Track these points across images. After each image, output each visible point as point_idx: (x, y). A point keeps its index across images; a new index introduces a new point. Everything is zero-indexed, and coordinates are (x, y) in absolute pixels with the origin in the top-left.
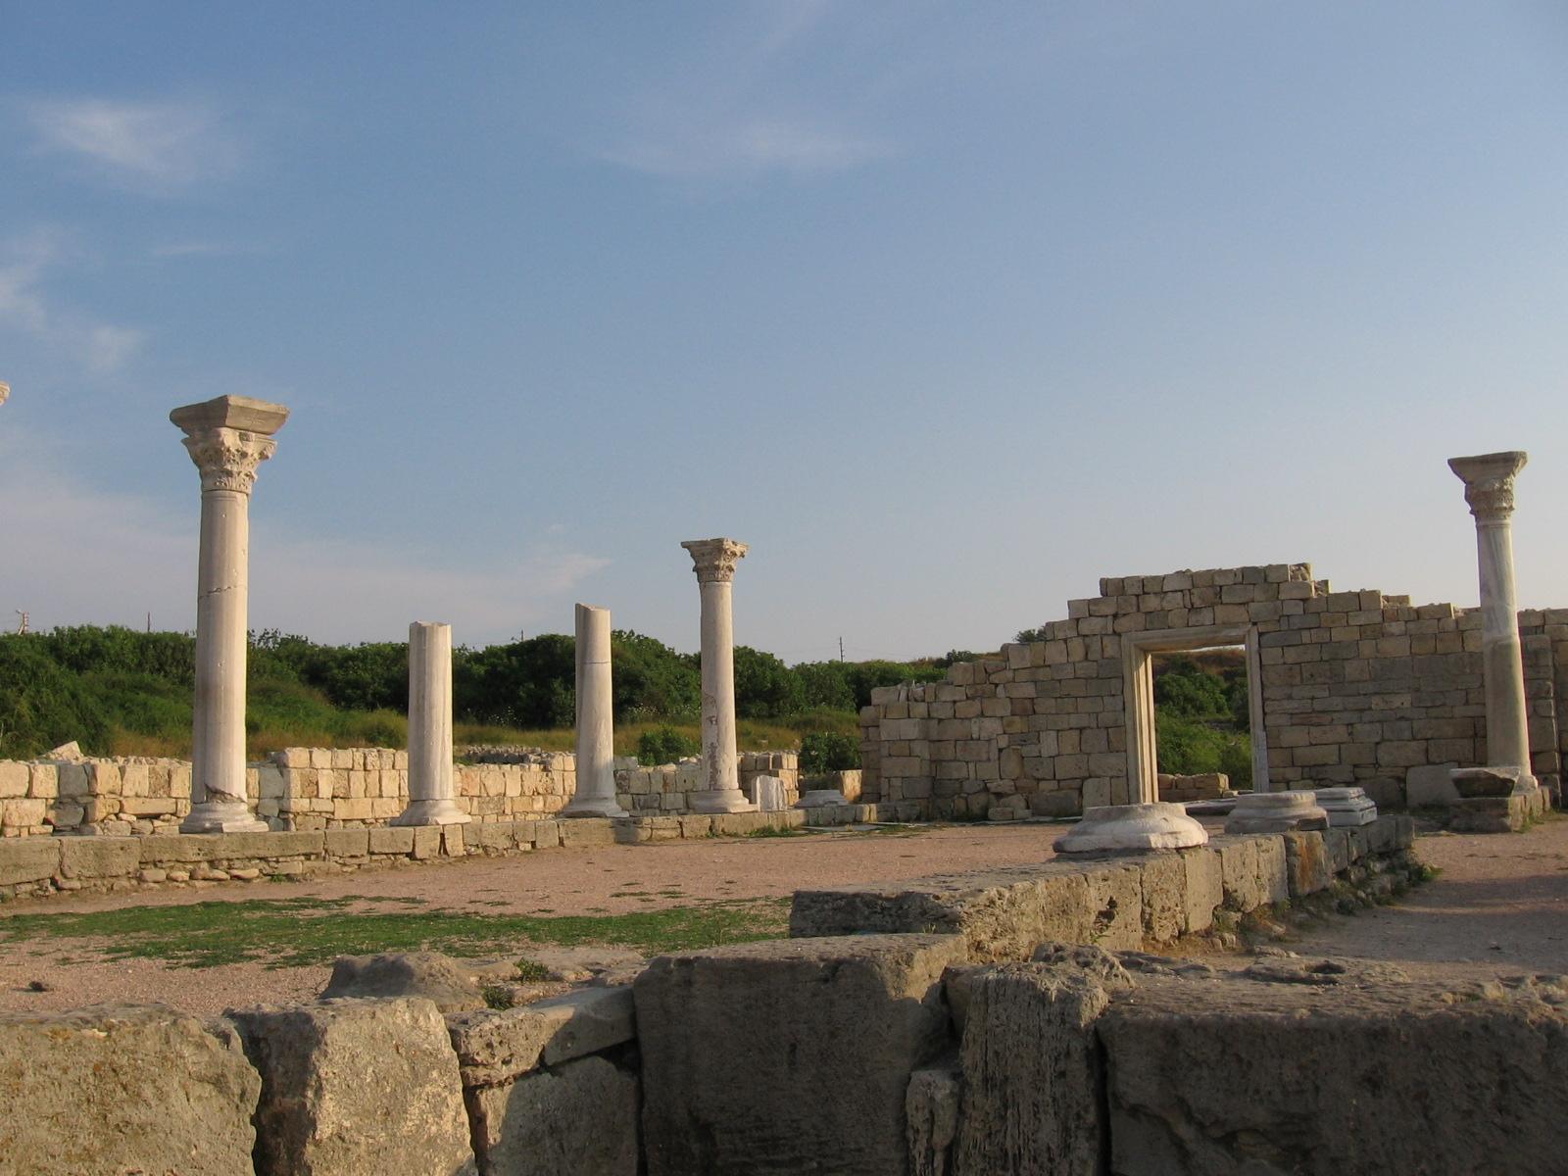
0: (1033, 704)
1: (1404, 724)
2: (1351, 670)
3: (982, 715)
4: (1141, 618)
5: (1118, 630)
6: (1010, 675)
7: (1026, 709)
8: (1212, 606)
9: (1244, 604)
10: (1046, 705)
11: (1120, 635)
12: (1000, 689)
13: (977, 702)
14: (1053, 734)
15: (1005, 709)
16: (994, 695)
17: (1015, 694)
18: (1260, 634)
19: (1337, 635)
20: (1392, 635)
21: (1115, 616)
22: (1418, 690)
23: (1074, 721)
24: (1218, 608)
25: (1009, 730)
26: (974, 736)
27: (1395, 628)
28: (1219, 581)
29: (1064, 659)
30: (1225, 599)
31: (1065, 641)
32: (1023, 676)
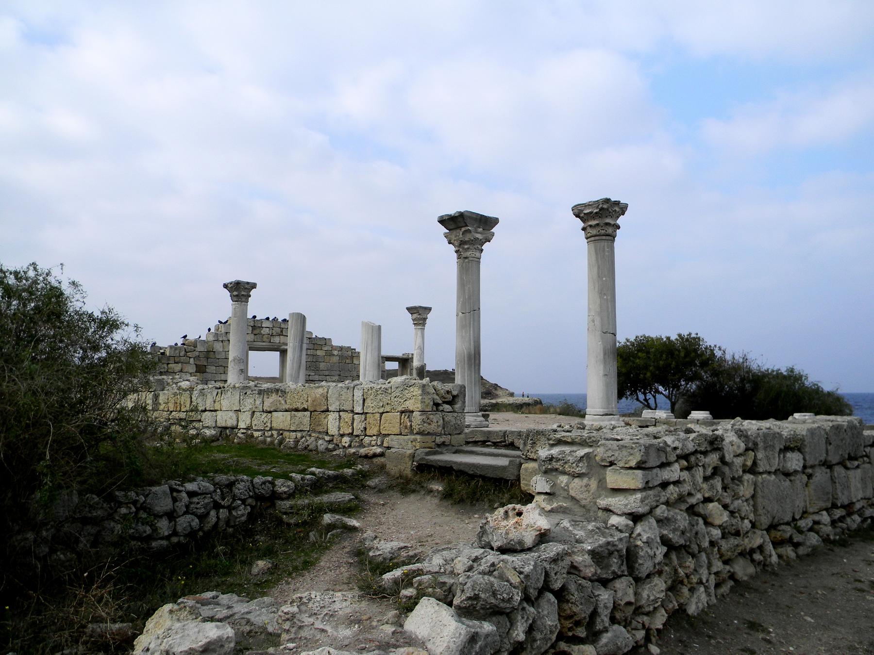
2: (322, 366)
3: (181, 371)
6: (197, 354)
13: (180, 365)
17: (198, 363)
19: (319, 353)
27: (336, 353)
29: (221, 350)
32: (202, 355)
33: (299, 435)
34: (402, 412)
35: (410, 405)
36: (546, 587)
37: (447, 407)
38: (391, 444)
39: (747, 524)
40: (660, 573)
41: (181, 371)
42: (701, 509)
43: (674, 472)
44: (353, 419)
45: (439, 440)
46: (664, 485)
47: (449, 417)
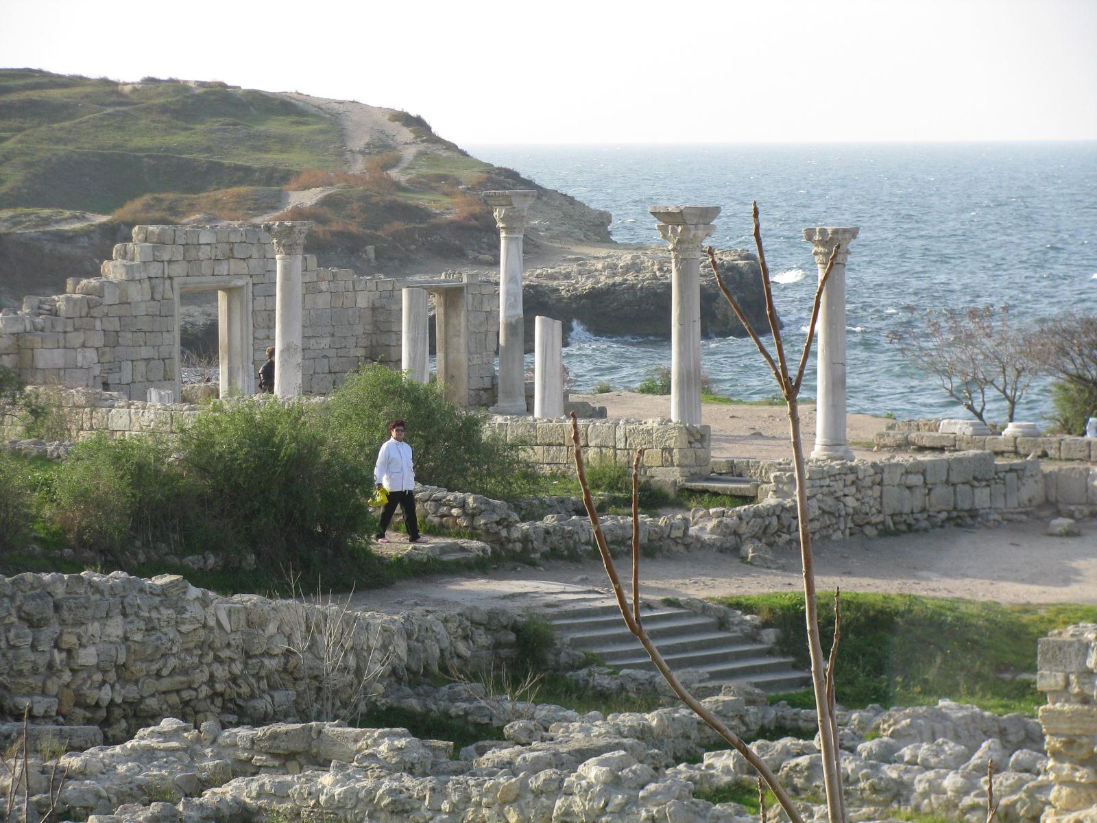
0: (118, 336)
1: (326, 360)
3: (83, 346)
4: (184, 264)
5: (172, 274)
7: (112, 340)
8: (228, 258)
9: (244, 259)
10: (126, 337)
11: (170, 278)
12: (98, 323)
14: (130, 362)
15: (98, 340)
16: (93, 328)
17: (109, 327)
18: (254, 284)
20: (322, 292)
21: (170, 262)
22: (333, 335)
23: (145, 352)
24: (232, 261)
25: (103, 360)
26: (79, 365)
28: (233, 238)
30: (236, 254)
31: (140, 281)
33: (555, 468)
34: (663, 449)
35: (672, 443)
36: (774, 513)
37: (697, 445)
38: (653, 474)
39: (874, 510)
40: (818, 520)
41: (83, 346)
42: (842, 499)
43: (827, 482)
44: (616, 454)
45: (693, 471)
46: (822, 487)
47: (700, 452)
